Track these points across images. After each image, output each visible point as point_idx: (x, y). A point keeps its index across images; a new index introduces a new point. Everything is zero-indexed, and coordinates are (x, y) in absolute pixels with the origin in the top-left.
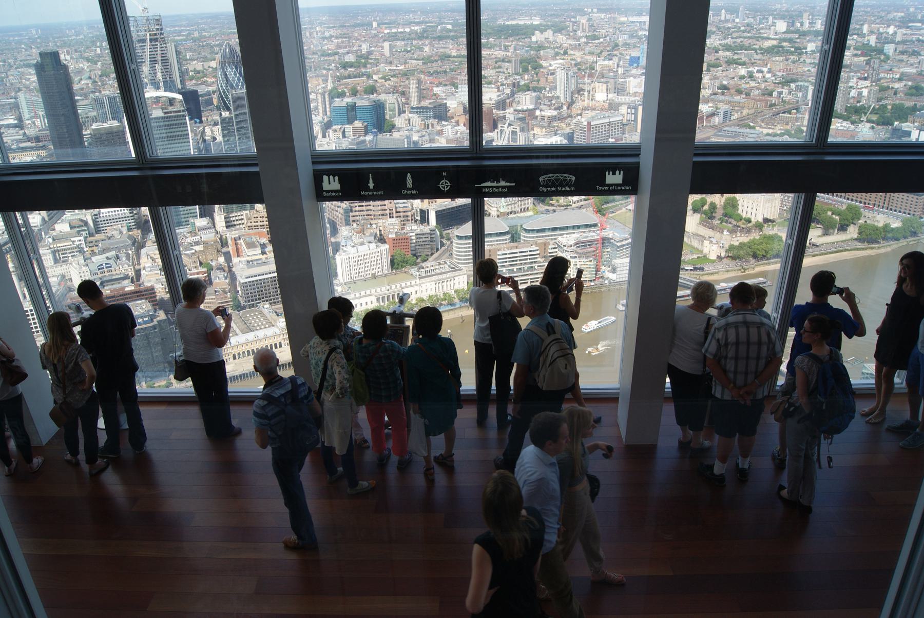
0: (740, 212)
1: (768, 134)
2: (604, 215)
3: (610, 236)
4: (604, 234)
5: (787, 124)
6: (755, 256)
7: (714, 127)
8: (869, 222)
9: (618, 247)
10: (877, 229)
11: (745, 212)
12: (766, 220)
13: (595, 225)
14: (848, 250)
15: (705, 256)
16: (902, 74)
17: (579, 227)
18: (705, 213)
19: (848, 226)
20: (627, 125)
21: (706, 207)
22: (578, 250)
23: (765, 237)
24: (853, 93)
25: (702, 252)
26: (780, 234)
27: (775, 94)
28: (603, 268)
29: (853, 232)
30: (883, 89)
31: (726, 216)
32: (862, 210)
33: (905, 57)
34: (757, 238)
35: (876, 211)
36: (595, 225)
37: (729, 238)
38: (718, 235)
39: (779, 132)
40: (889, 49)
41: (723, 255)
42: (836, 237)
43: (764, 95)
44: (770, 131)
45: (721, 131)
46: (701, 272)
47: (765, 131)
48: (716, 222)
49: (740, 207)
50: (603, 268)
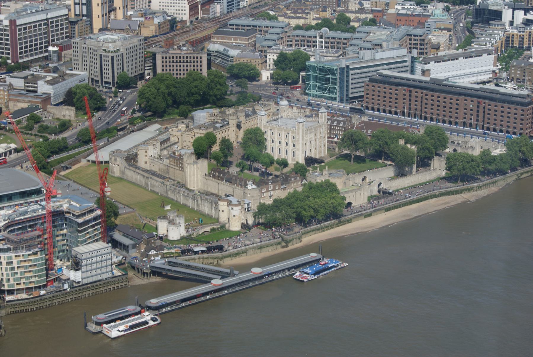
0: (269, 151)
1: (298, 27)
2: (50, 173)
3: (65, 207)
4: (53, 205)
5: (324, 10)
6: (300, 220)
7: (215, 19)
8: (459, 150)
9: (80, 225)
10: (472, 159)
11: (276, 151)
12: (310, 161)
13: (38, 192)
14: (435, 196)
15: (223, 227)
17: (10, 197)
18: (216, 158)
19: (430, 158)
20: (76, 22)
21: (216, 148)
22: (12, 236)
23: (311, 187)
25: (217, 220)
26: (332, 180)
28: (58, 263)
29: (438, 168)
31: (248, 159)
32: (448, 133)
34: (300, 189)
35: (468, 133)
36: (38, 192)
37: (256, 193)
38: (238, 191)
39: (314, 23)
41: (250, 222)
42: (416, 178)
44: (301, 22)
45: (225, 26)
46: (220, 254)
47: (294, 22)
48: (234, 170)
49: (268, 144)
50: (58, 263)
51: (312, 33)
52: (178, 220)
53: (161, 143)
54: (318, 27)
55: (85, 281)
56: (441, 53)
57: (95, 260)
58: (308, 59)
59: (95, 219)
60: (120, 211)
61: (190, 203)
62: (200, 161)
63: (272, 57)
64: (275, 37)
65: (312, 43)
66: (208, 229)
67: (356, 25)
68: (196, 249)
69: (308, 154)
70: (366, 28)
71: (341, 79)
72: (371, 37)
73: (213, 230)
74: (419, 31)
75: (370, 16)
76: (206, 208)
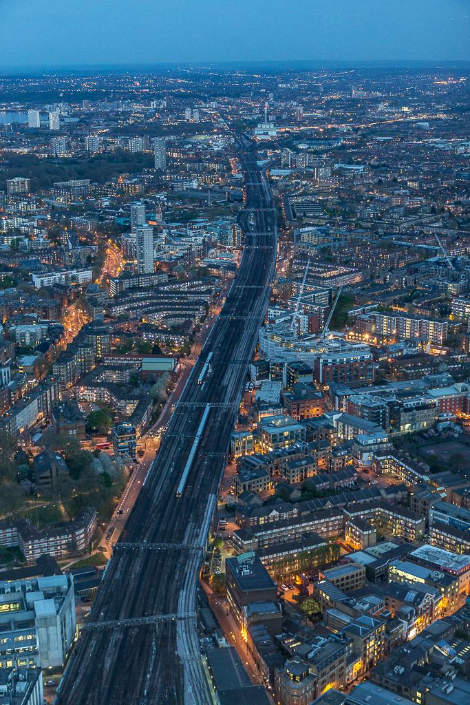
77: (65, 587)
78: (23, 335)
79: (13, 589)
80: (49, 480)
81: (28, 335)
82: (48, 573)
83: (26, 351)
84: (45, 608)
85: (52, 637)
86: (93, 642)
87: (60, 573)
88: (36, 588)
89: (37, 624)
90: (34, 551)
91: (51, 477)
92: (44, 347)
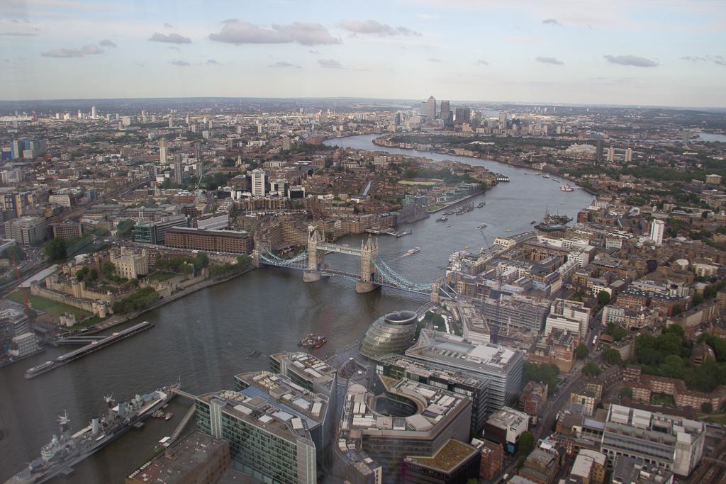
1: (129, 207)
16: (217, 151)
24: (187, 168)
25: (92, 313)
27: (129, 174)
30: (206, 163)
33: (217, 140)
40: (205, 134)
43: (120, 176)
44: (130, 204)
47: (127, 204)
51: (136, 209)
52: (70, 316)
53: (59, 275)
54: (139, 206)
55: (22, 355)
56: (202, 216)
57: (26, 343)
58: (135, 223)
59: (24, 321)
60: (39, 314)
61: (77, 305)
62: (81, 283)
63: (116, 223)
64: (117, 213)
65: (136, 215)
66: (88, 318)
67: (159, 203)
68: (83, 330)
69: (138, 273)
70: (164, 205)
71: (153, 232)
72: (167, 210)
73: (91, 319)
74: (191, 205)
75: (166, 198)
76: (86, 307)
77: (700, 430)
78: (701, 270)
79: (666, 420)
80: (700, 362)
81: (703, 271)
82: (689, 418)
83: (701, 280)
84: (683, 438)
85: (685, 458)
86: (711, 471)
87: (697, 420)
88: (680, 424)
89: (677, 445)
90: (684, 400)
91: (703, 360)
92: (713, 280)
